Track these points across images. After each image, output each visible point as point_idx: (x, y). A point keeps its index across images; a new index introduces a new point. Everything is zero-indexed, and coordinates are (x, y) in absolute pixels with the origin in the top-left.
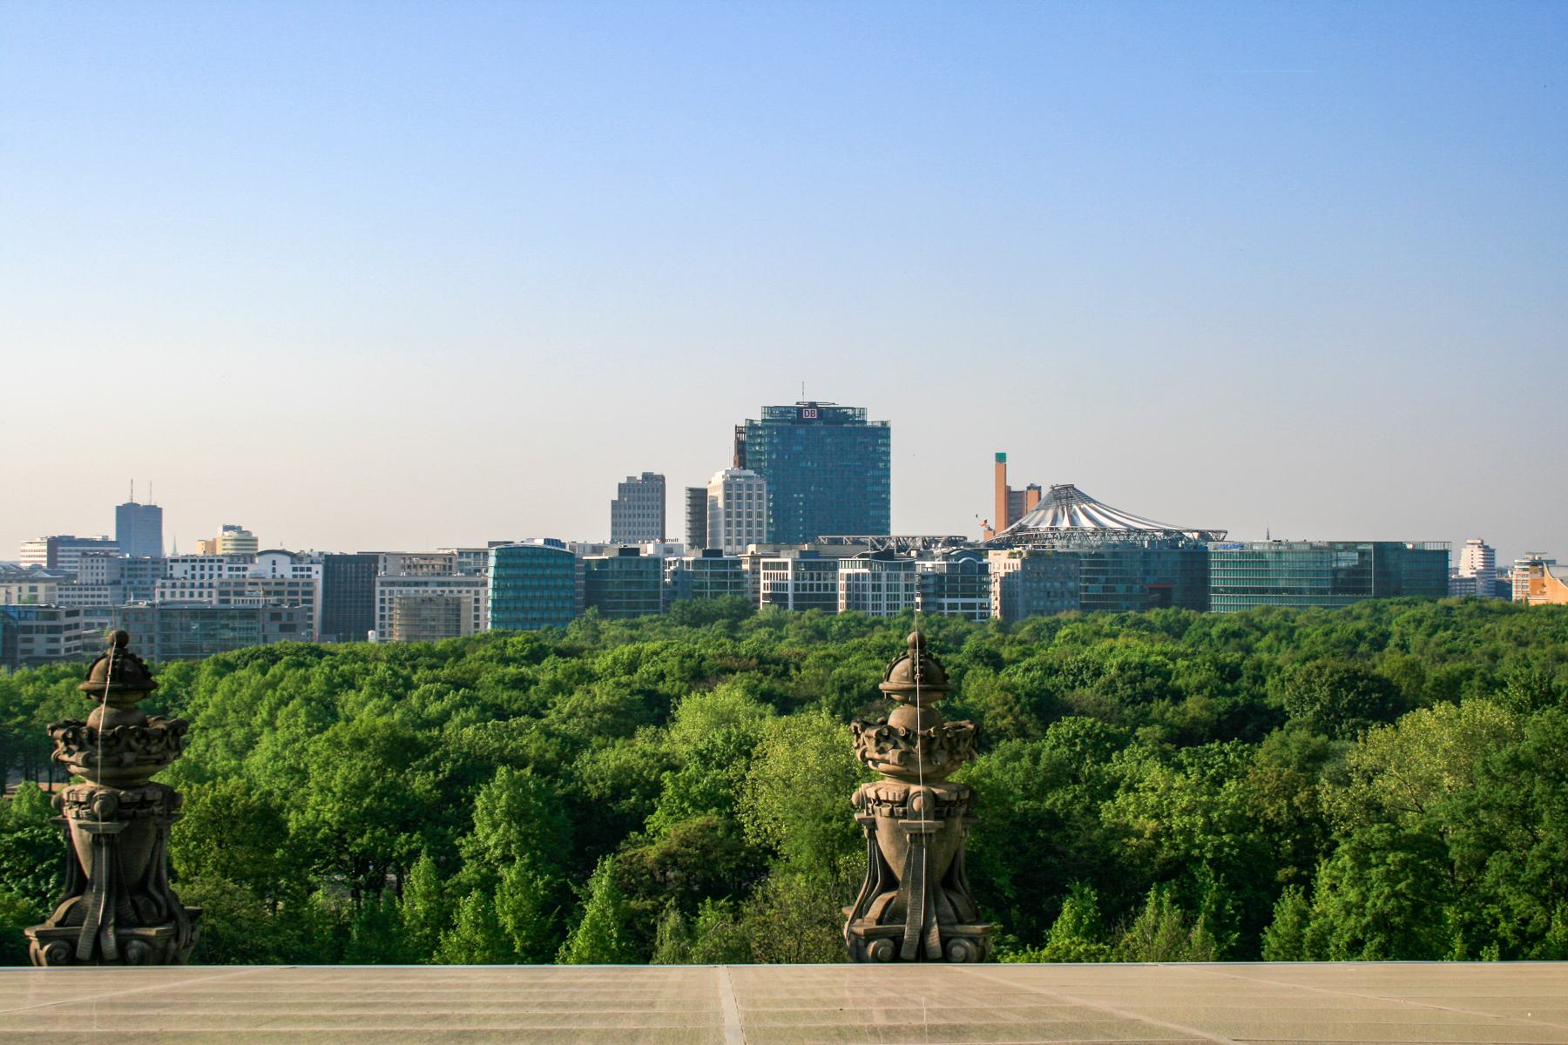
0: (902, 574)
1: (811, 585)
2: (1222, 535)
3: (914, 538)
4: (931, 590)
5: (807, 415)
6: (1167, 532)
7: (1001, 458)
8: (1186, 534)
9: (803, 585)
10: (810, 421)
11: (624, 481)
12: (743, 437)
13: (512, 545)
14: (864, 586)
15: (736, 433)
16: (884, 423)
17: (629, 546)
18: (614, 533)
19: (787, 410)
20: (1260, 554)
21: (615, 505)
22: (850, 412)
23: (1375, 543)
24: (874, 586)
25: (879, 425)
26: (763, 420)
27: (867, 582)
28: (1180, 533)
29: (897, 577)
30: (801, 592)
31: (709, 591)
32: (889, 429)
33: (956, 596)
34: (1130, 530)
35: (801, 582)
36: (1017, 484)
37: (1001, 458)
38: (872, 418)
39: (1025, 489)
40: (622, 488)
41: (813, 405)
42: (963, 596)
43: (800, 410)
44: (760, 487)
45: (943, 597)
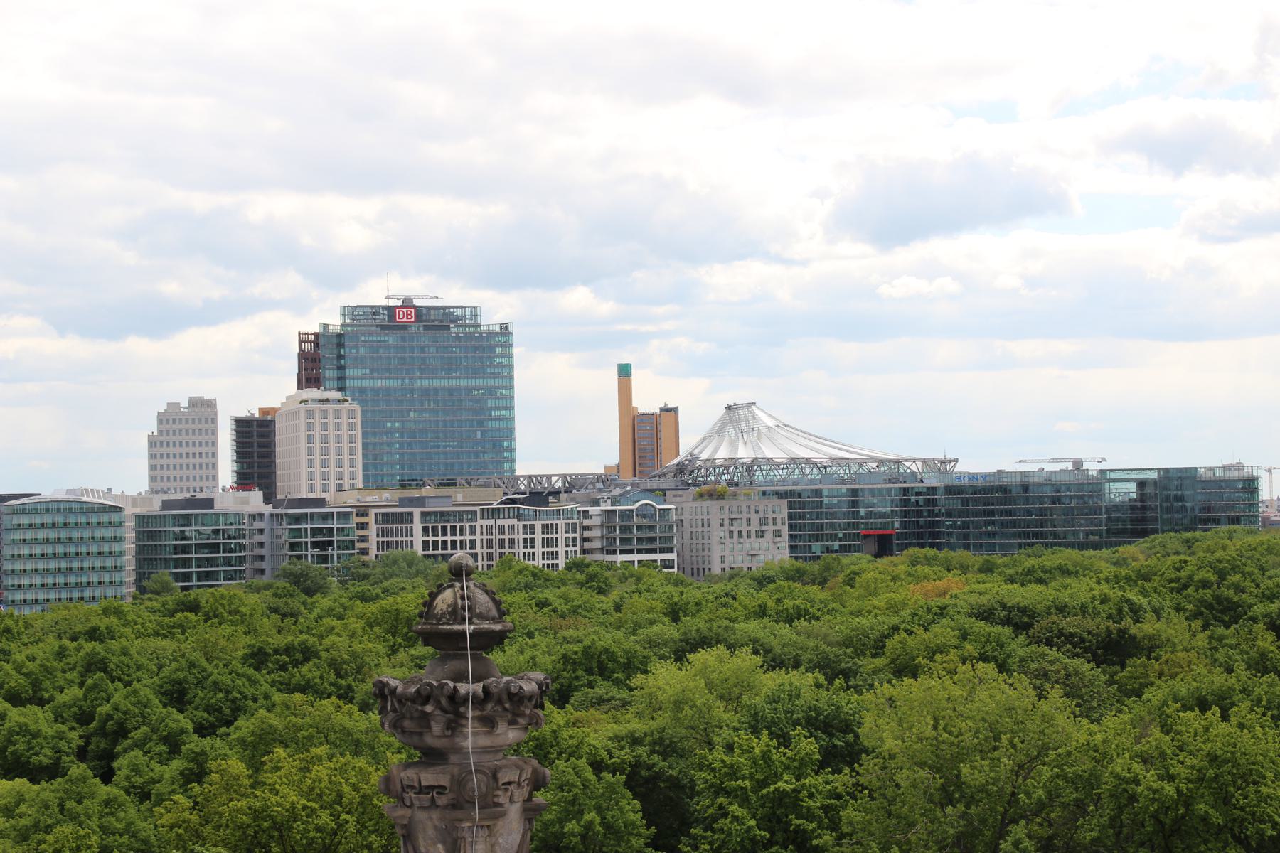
0: (562, 524)
1: (444, 542)
2: (953, 464)
3: (549, 477)
4: (597, 544)
5: (401, 316)
6: (881, 462)
7: (624, 371)
8: (908, 464)
9: (461, 541)
10: (404, 327)
11: (163, 408)
12: (307, 347)
13: (36, 499)
14: (511, 541)
15: (301, 342)
16: (504, 327)
17: (199, 496)
18: (152, 479)
19: (375, 310)
20: (1004, 489)
21: (153, 443)
22: (458, 312)
23: (1159, 469)
24: (525, 541)
25: (497, 329)
26: (342, 325)
27: (516, 537)
28: (898, 462)
29: (555, 528)
30: (431, 552)
31: (335, 553)
32: (511, 334)
33: (631, 552)
34: (795, 461)
35: (468, 538)
36: (646, 401)
37: (624, 371)
38: (490, 320)
39: (658, 411)
40: (162, 419)
41: (407, 303)
42: (639, 551)
43: (391, 310)
44: (352, 414)
45: (614, 552)
